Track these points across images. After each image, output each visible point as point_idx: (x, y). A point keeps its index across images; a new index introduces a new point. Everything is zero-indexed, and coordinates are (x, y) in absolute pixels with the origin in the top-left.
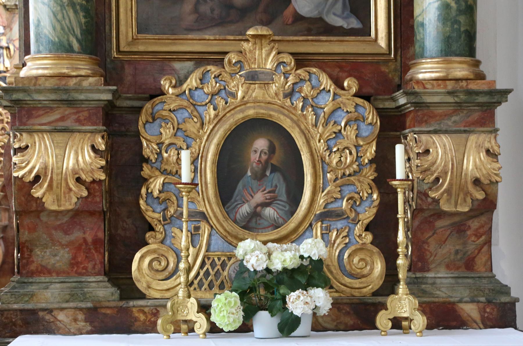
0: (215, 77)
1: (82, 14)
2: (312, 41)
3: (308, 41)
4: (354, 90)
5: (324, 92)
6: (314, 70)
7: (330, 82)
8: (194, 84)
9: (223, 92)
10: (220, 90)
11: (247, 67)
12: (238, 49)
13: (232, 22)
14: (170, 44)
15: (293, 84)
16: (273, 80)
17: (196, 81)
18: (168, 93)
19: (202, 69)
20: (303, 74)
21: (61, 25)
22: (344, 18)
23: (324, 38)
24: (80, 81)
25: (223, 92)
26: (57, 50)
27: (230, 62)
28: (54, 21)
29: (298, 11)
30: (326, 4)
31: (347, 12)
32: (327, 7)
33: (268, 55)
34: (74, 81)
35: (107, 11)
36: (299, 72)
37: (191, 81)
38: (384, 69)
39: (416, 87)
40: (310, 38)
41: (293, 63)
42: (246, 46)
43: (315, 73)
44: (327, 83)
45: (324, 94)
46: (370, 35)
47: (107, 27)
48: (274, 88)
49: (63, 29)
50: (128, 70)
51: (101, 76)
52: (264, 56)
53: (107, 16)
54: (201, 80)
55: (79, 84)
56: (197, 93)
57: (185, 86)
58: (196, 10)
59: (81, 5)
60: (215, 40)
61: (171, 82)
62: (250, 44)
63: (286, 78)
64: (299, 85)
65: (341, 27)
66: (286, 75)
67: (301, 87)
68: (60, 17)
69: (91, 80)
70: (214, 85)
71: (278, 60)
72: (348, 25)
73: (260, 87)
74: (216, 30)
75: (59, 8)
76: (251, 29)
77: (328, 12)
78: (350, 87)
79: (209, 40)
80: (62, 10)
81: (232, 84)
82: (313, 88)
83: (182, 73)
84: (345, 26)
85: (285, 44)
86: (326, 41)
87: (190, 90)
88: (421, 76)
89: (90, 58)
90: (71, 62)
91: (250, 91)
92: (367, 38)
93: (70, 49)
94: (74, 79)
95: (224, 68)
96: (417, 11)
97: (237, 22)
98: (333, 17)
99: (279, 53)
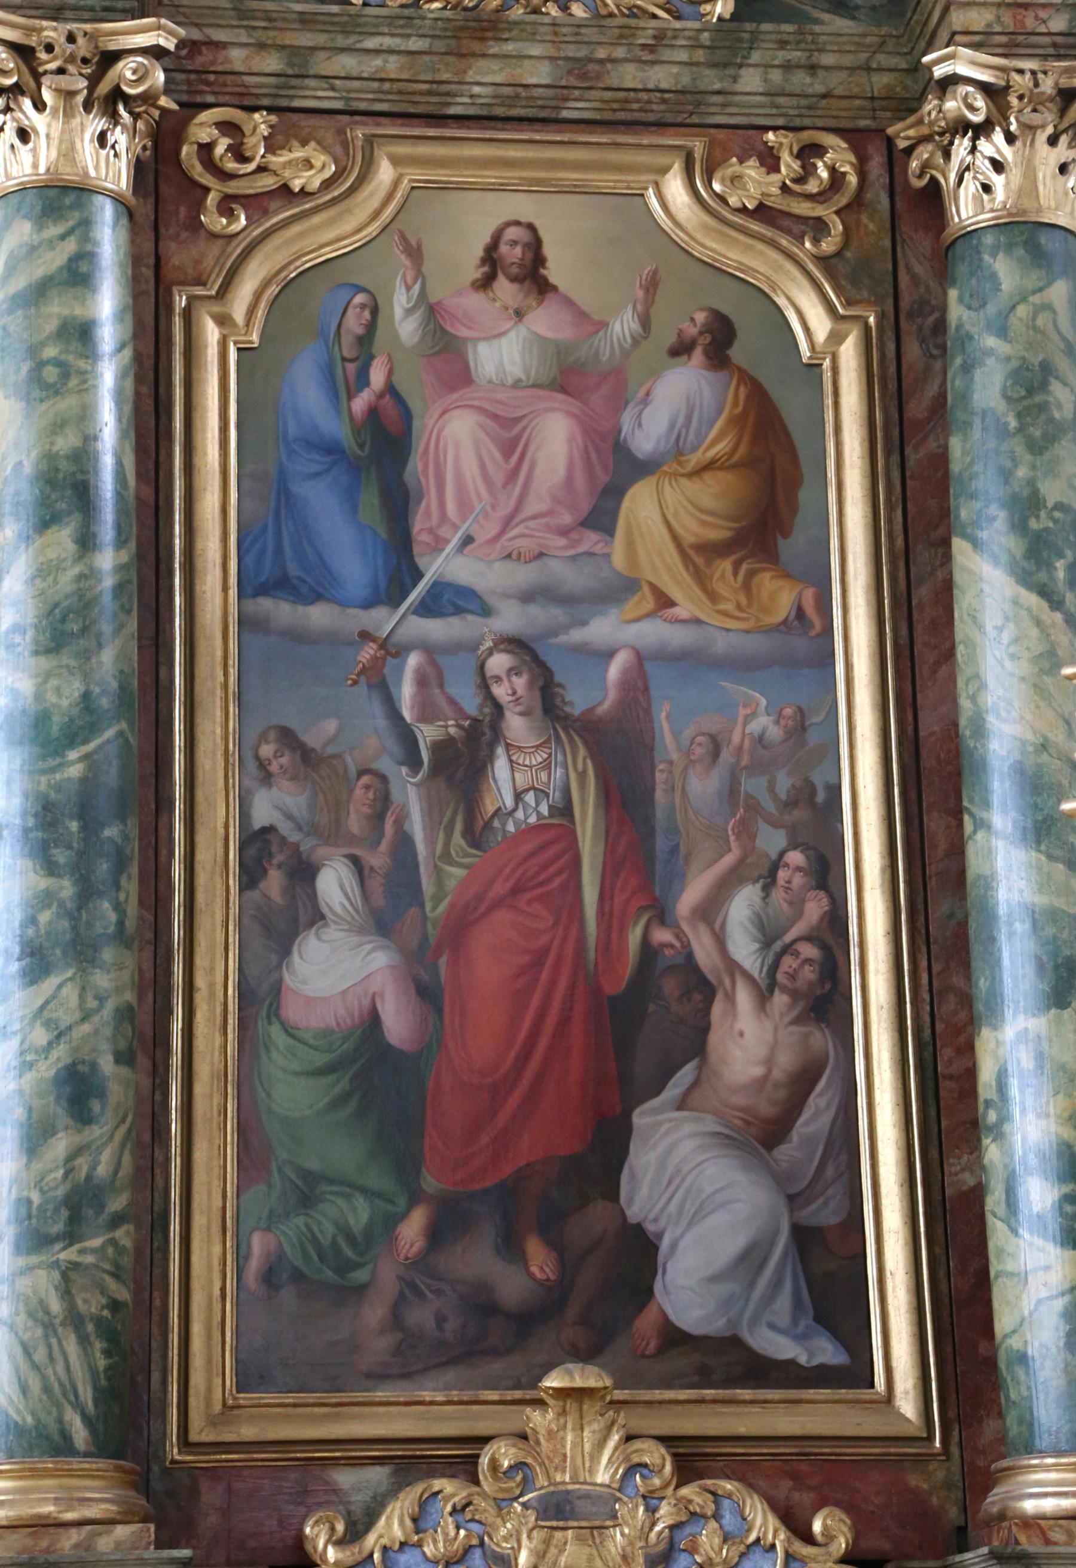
0: (454, 1511)
1: (98, 1345)
2: (714, 1401)
3: (702, 1401)
4: (841, 1544)
5: (758, 1550)
6: (729, 1486)
7: (773, 1521)
8: (398, 1533)
9: (478, 1553)
10: (468, 1550)
11: (541, 1481)
12: (514, 1426)
13: (494, 1352)
14: (326, 1416)
15: (672, 1528)
16: (614, 1517)
17: (402, 1523)
18: (325, 1561)
19: (419, 1488)
20: (697, 1499)
21: (44, 1378)
22: (801, 1338)
23: (746, 1394)
24: (93, 1535)
25: (478, 1553)
26: (29, 1451)
27: (494, 1465)
28: (24, 1366)
29: (672, 1317)
30: (747, 1300)
31: (806, 1322)
32: (752, 1306)
33: (600, 1445)
34: (74, 1536)
35: (155, 1331)
36: (685, 1491)
37: (389, 1524)
38: (914, 1480)
39: (1022, 1538)
40: (709, 1393)
41: (668, 1468)
42: (539, 1420)
43: (729, 1496)
44: (765, 1524)
45: (757, 1555)
46: (872, 1385)
47: (156, 1376)
48: (618, 1538)
49: (47, 1389)
50: (211, 1496)
51: (145, 1520)
52: (587, 1447)
53: (154, 1345)
54: (414, 1520)
55: (87, 1546)
56: (403, 1558)
57: (371, 1539)
58: (396, 1319)
59: (99, 1321)
60: (449, 1403)
61: (333, 1529)
62: (550, 1415)
63: (651, 1510)
64: (688, 1530)
65: (792, 1363)
66: (651, 1500)
67: (695, 1536)
68: (40, 1356)
69: (121, 1532)
70: (452, 1533)
71: (627, 1459)
72: (811, 1355)
73: (579, 1539)
74: (450, 1375)
75: (39, 1332)
76: (554, 1374)
77: (754, 1321)
78: (829, 1537)
79: (432, 1403)
80: (46, 1336)
81: (503, 1532)
82: (726, 1538)
83: (359, 1500)
84: (803, 1360)
85: (640, 1410)
86: (753, 1402)
87: (385, 1549)
88: (1029, 1506)
89: (118, 1468)
90: (65, 1481)
91: (553, 1551)
92: (864, 1394)
93: (62, 1446)
94: (73, 1531)
95: (476, 1482)
96: (1003, 1322)
97: (508, 1351)
98: (768, 1333)
99: (629, 1438)
